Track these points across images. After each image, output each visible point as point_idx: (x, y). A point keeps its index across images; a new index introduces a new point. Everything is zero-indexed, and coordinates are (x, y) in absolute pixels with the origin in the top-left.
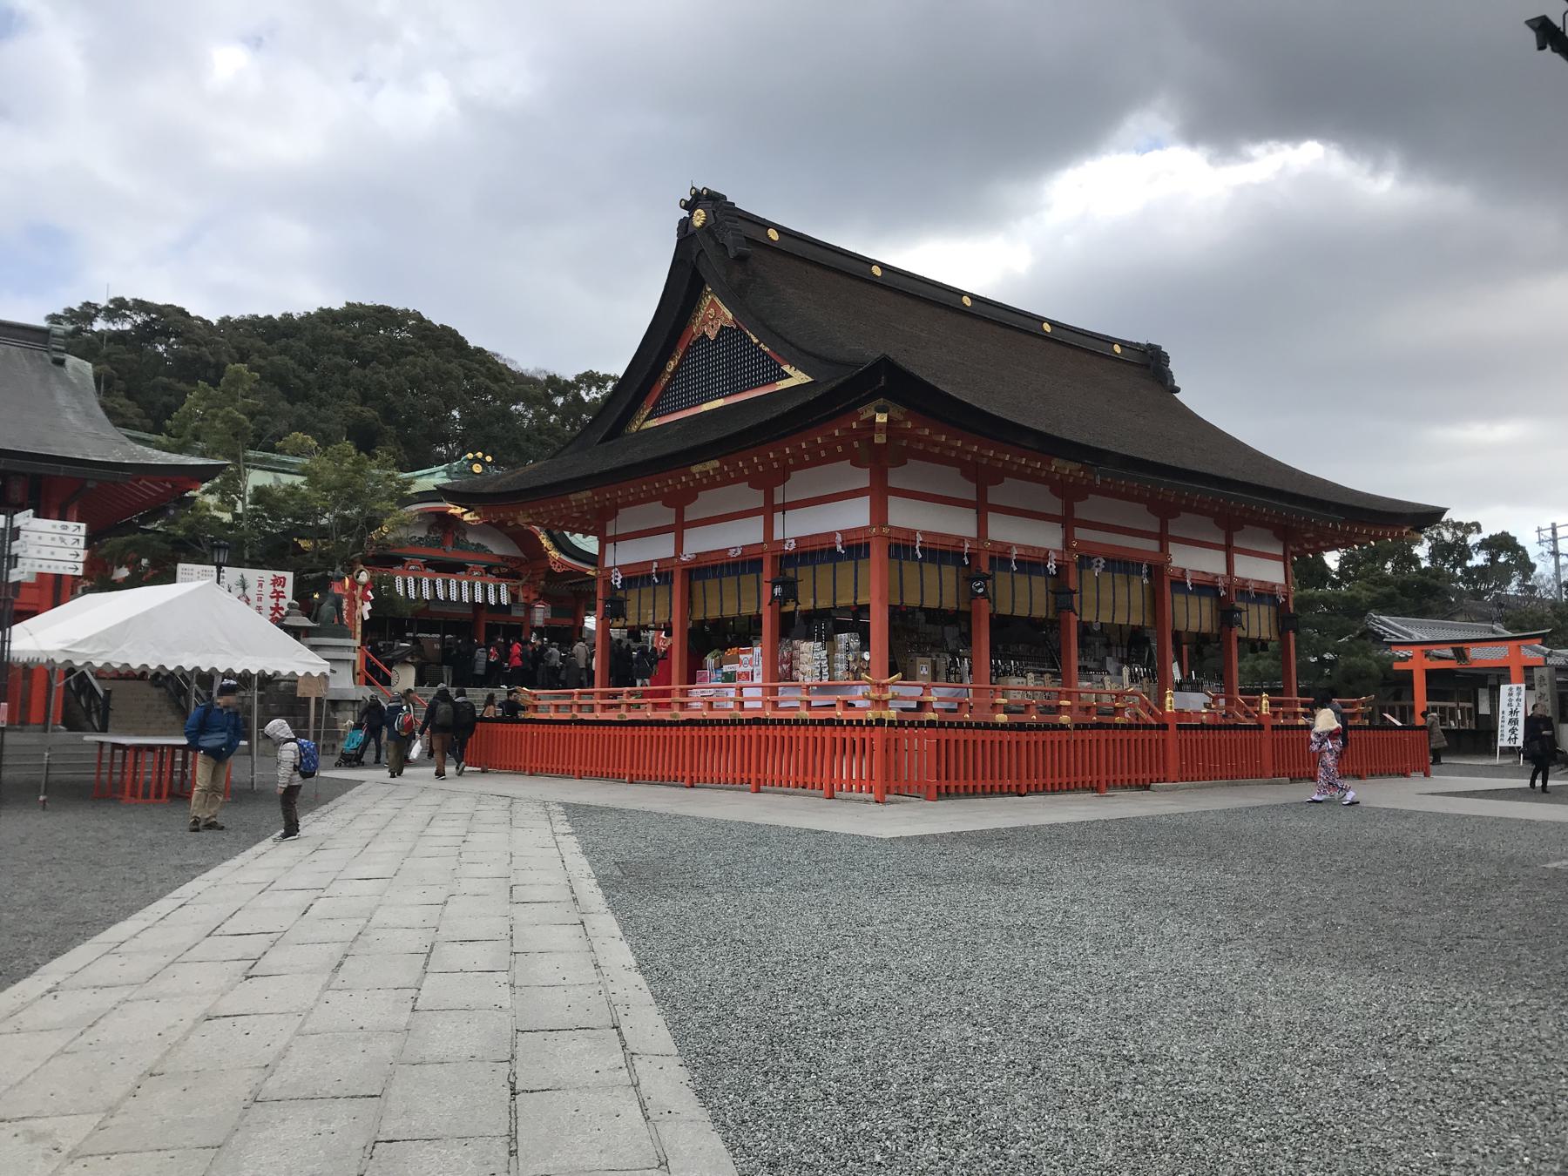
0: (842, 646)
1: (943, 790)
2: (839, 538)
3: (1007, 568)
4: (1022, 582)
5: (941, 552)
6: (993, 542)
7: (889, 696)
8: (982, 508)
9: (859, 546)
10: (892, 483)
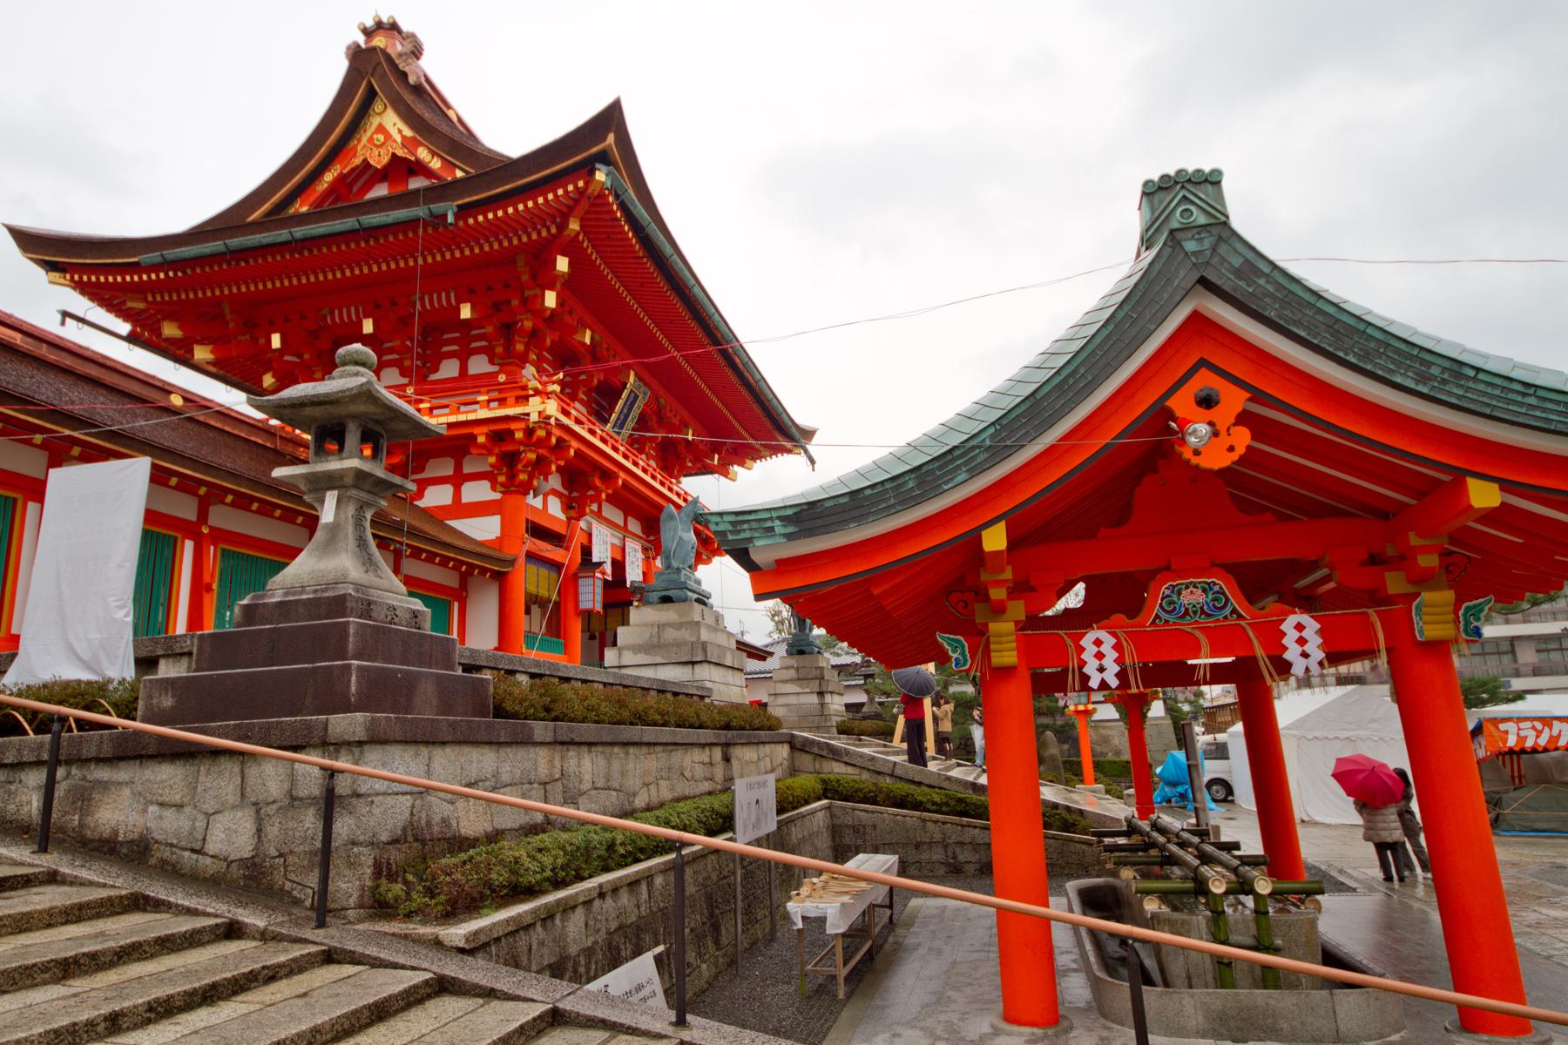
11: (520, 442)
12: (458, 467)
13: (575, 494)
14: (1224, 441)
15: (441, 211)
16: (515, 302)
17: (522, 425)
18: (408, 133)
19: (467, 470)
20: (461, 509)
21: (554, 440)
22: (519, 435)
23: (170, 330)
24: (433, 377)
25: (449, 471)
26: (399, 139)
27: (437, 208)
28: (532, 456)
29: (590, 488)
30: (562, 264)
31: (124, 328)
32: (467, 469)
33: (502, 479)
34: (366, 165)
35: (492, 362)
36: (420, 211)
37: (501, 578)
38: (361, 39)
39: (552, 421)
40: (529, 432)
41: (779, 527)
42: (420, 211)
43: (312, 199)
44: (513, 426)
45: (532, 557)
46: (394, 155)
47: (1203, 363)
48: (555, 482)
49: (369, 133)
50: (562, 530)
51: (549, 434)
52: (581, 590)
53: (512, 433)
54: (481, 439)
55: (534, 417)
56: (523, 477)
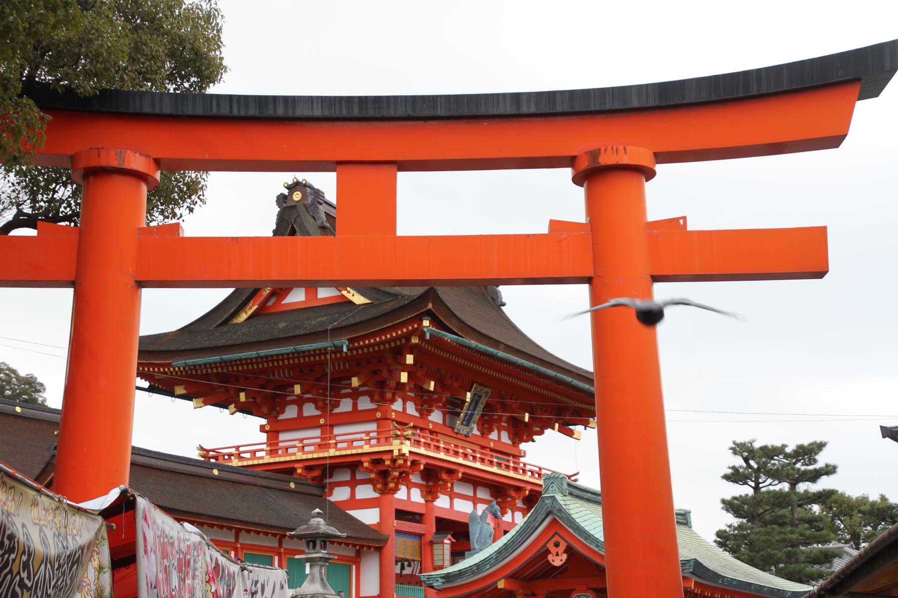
11: (388, 466)
12: (353, 475)
13: (430, 483)
14: (559, 558)
16: (385, 373)
19: (359, 477)
20: (355, 503)
21: (409, 463)
22: (388, 463)
23: (180, 390)
24: (336, 411)
25: (347, 477)
27: (337, 343)
28: (396, 474)
29: (439, 480)
30: (410, 359)
31: (146, 384)
32: (359, 477)
37: (379, 549)
38: (286, 192)
39: (407, 455)
41: (440, 580)
44: (384, 457)
45: (398, 532)
47: (556, 533)
48: (415, 478)
50: (422, 511)
51: (406, 461)
52: (435, 552)
53: (383, 461)
54: (366, 465)
55: (396, 453)
56: (392, 485)
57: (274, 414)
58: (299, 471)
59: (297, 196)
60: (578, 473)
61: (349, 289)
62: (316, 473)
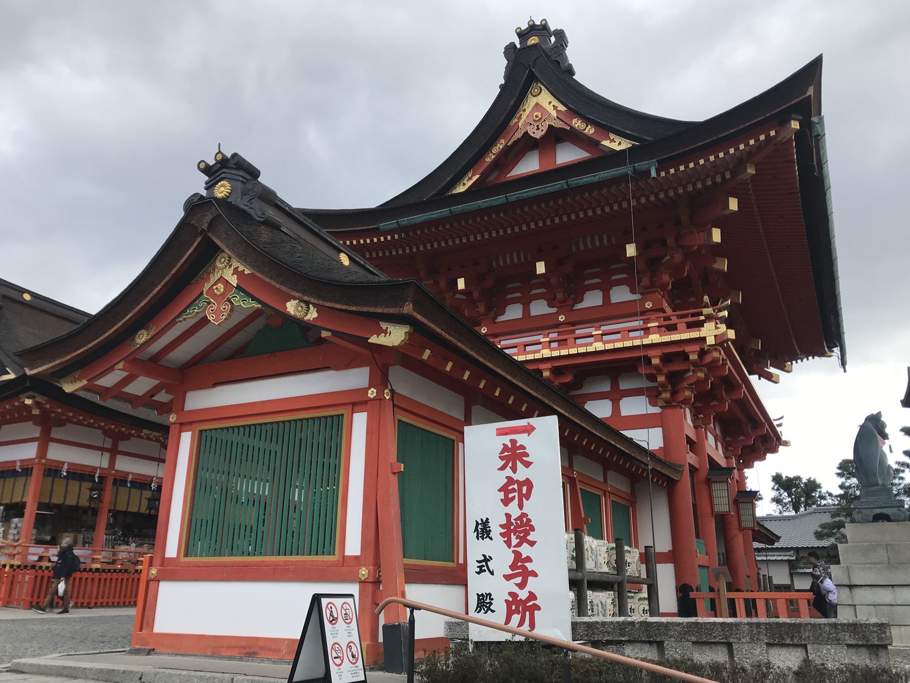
0: (13, 525)
1: (34, 604)
2: (66, 467)
3: (126, 486)
4: (136, 493)
5: (79, 474)
6: (118, 471)
7: (15, 552)
8: (114, 452)
9: (27, 469)
10: (53, 435)
12: (615, 384)
15: (644, 168)
17: (697, 348)
18: (562, 108)
22: (693, 357)
26: (554, 114)
33: (666, 395)
34: (526, 133)
35: (633, 291)
36: (627, 169)
40: (702, 353)
42: (627, 169)
43: (481, 170)
44: (688, 349)
46: (550, 126)
49: (528, 112)
52: (715, 494)
55: (711, 341)
57: (492, 315)
58: (546, 374)
59: (533, 40)
60: (782, 418)
61: (612, 136)
62: (568, 379)
